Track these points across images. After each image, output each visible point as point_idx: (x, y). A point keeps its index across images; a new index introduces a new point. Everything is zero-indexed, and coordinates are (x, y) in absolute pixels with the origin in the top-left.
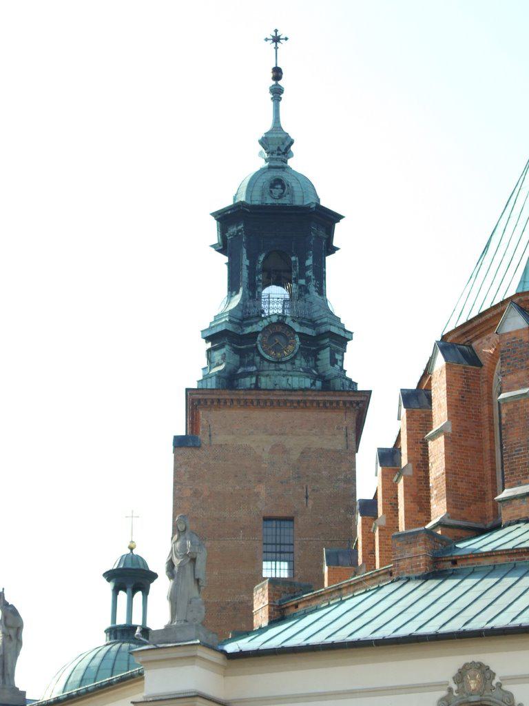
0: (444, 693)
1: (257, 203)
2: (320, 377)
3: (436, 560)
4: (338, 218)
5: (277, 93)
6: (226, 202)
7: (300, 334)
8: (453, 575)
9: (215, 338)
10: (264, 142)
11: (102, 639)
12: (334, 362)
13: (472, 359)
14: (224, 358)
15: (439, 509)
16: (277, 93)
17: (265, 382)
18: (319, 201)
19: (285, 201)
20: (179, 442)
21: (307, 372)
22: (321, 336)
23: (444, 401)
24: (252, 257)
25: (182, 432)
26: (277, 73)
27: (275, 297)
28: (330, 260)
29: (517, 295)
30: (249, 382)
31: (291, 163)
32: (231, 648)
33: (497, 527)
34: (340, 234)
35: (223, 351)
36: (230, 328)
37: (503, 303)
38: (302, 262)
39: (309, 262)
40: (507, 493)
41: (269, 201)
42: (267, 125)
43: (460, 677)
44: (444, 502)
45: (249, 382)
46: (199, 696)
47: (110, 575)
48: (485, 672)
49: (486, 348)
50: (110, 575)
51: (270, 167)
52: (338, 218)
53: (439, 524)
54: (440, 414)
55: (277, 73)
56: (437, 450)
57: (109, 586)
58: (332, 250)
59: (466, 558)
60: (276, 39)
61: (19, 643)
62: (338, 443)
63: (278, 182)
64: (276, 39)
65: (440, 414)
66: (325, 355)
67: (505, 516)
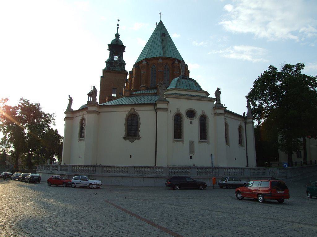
0: (128, 112)
1: (114, 43)
3: (130, 94)
4: (125, 47)
5: (118, 28)
6: (110, 43)
7: (119, 63)
9: (107, 62)
11: (87, 103)
12: (123, 67)
13: (139, 67)
14: (108, 65)
15: (133, 88)
16: (118, 28)
19: (118, 44)
22: (122, 64)
23: (134, 73)
25: (102, 75)
26: (118, 25)
27: (116, 58)
28: (124, 53)
29: (145, 59)
31: (119, 38)
33: (140, 90)
35: (109, 64)
37: (144, 59)
38: (120, 53)
39: (121, 53)
40: (141, 86)
41: (116, 44)
42: (116, 33)
43: (131, 110)
44: (133, 87)
45: (112, 69)
46: (95, 111)
47: (88, 94)
48: (134, 110)
49: (140, 66)
50: (88, 94)
52: (125, 47)
53: (133, 90)
54: (134, 75)
55: (118, 25)
56: (133, 79)
57: (88, 96)
58: (124, 51)
59: (134, 94)
60: (118, 20)
61: (72, 103)
63: (117, 41)
64: (118, 20)
65: (134, 75)
67: (141, 89)
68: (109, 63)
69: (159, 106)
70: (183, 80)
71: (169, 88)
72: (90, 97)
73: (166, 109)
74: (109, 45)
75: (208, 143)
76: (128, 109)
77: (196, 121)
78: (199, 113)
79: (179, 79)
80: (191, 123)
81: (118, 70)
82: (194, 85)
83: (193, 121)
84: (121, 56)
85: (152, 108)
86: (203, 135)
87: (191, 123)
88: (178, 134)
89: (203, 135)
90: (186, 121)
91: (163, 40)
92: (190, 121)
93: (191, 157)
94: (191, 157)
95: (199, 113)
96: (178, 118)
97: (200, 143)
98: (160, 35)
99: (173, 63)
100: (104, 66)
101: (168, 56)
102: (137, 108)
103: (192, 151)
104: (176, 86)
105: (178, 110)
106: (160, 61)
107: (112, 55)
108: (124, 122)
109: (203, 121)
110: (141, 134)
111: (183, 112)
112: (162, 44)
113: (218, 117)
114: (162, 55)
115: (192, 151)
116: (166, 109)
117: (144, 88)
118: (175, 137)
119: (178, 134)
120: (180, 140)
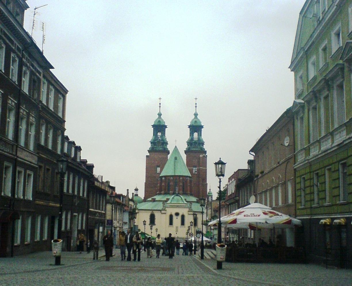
2: (164, 148)
8: (155, 202)
10: (158, 114)
17: (157, 149)
18: (165, 123)
20: (147, 156)
21: (162, 148)
24: (156, 131)
27: (159, 134)
30: (155, 149)
31: (161, 116)
32: (139, 209)
34: (167, 127)
36: (153, 142)
41: (158, 124)
45: (155, 149)
48: (153, 212)
51: (158, 118)
55: (160, 104)
57: (134, 190)
60: (160, 99)
62: (165, 157)
63: (159, 121)
64: (160, 99)
66: (164, 145)
68: (153, 143)
69: (162, 212)
70: (176, 197)
71: (168, 202)
72: (136, 191)
73: (165, 213)
74: (153, 126)
75: (185, 227)
76: (151, 211)
77: (179, 218)
78: (181, 214)
79: (173, 197)
80: (177, 218)
81: (161, 149)
82: (180, 200)
83: (178, 218)
84: (164, 134)
85: (160, 212)
86: (183, 223)
87: (177, 218)
88: (171, 223)
89: (183, 223)
90: (175, 217)
91: (175, 162)
92: (176, 217)
93: (176, 233)
94: (176, 233)
95: (181, 214)
96: (171, 217)
97: (181, 227)
98: (174, 158)
99: (179, 179)
100: (149, 146)
101: (176, 175)
102: (154, 212)
103: (177, 231)
104: (171, 202)
105: (171, 213)
106: (172, 178)
107: (155, 134)
108: (149, 217)
109: (183, 217)
110: (156, 223)
111: (173, 214)
112: (174, 165)
113: (189, 216)
114: (173, 175)
115: (177, 231)
116: (165, 213)
117: (163, 194)
118: (170, 225)
119: (171, 223)
120: (171, 226)
